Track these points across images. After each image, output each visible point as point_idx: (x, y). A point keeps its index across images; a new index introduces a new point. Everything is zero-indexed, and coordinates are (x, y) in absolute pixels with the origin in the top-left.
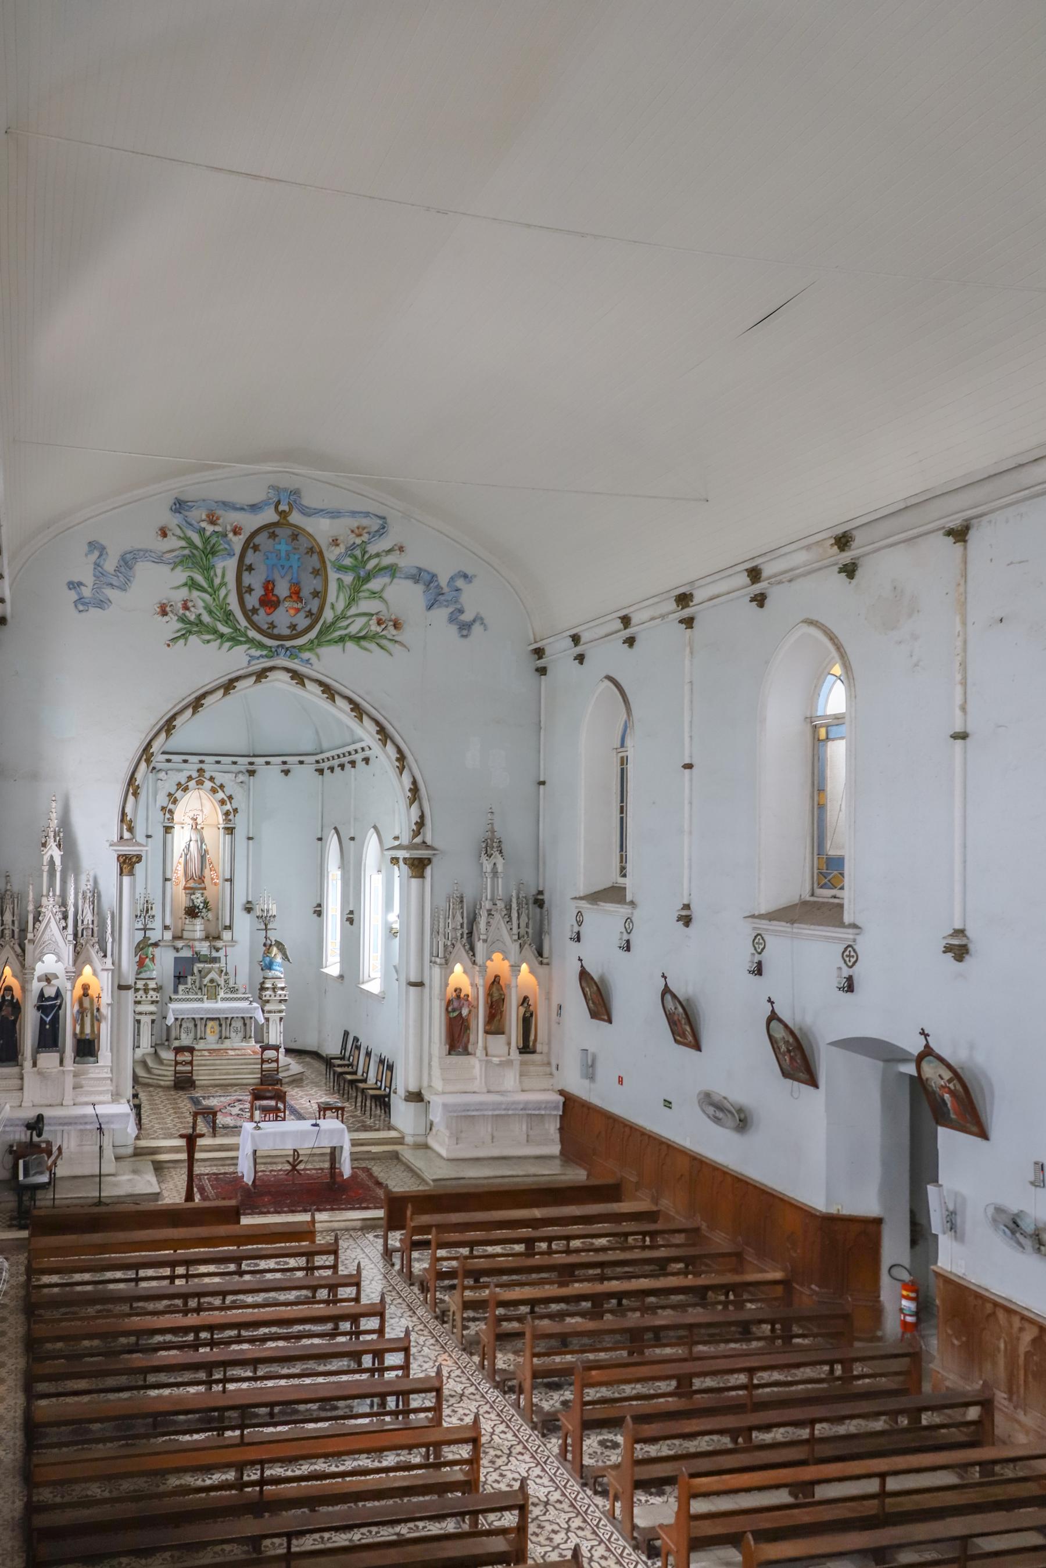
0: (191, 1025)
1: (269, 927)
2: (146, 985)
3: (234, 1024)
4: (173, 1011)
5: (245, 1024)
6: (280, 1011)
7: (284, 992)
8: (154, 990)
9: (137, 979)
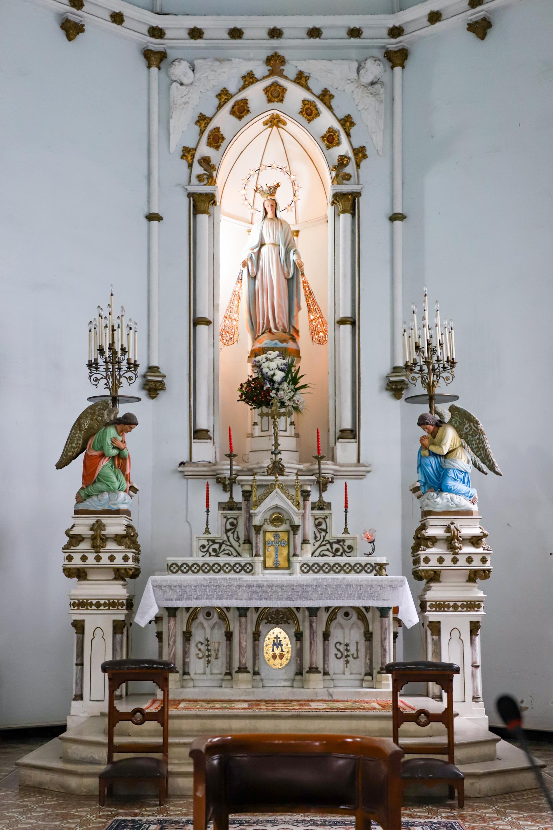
0: (218, 636)
1: (437, 390)
2: (98, 526)
3: (337, 635)
4: (157, 587)
5: (368, 636)
6: (472, 605)
7: (480, 550)
8: (119, 539)
9: (77, 512)
